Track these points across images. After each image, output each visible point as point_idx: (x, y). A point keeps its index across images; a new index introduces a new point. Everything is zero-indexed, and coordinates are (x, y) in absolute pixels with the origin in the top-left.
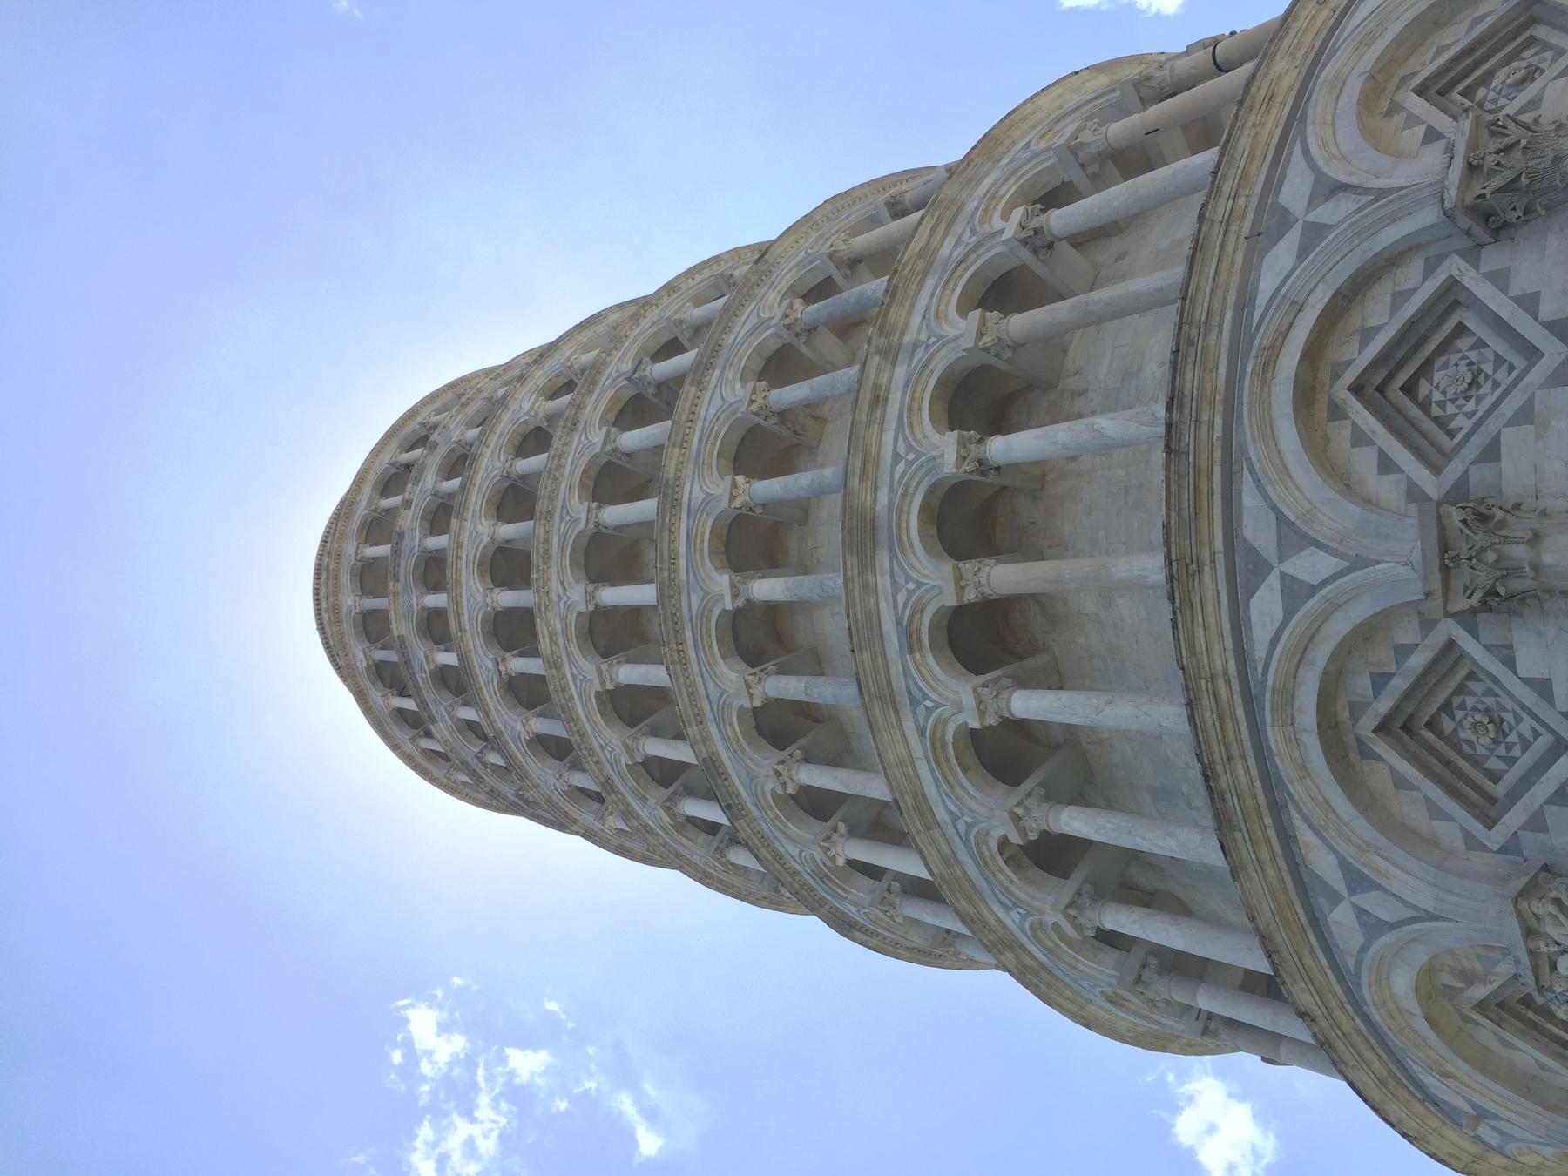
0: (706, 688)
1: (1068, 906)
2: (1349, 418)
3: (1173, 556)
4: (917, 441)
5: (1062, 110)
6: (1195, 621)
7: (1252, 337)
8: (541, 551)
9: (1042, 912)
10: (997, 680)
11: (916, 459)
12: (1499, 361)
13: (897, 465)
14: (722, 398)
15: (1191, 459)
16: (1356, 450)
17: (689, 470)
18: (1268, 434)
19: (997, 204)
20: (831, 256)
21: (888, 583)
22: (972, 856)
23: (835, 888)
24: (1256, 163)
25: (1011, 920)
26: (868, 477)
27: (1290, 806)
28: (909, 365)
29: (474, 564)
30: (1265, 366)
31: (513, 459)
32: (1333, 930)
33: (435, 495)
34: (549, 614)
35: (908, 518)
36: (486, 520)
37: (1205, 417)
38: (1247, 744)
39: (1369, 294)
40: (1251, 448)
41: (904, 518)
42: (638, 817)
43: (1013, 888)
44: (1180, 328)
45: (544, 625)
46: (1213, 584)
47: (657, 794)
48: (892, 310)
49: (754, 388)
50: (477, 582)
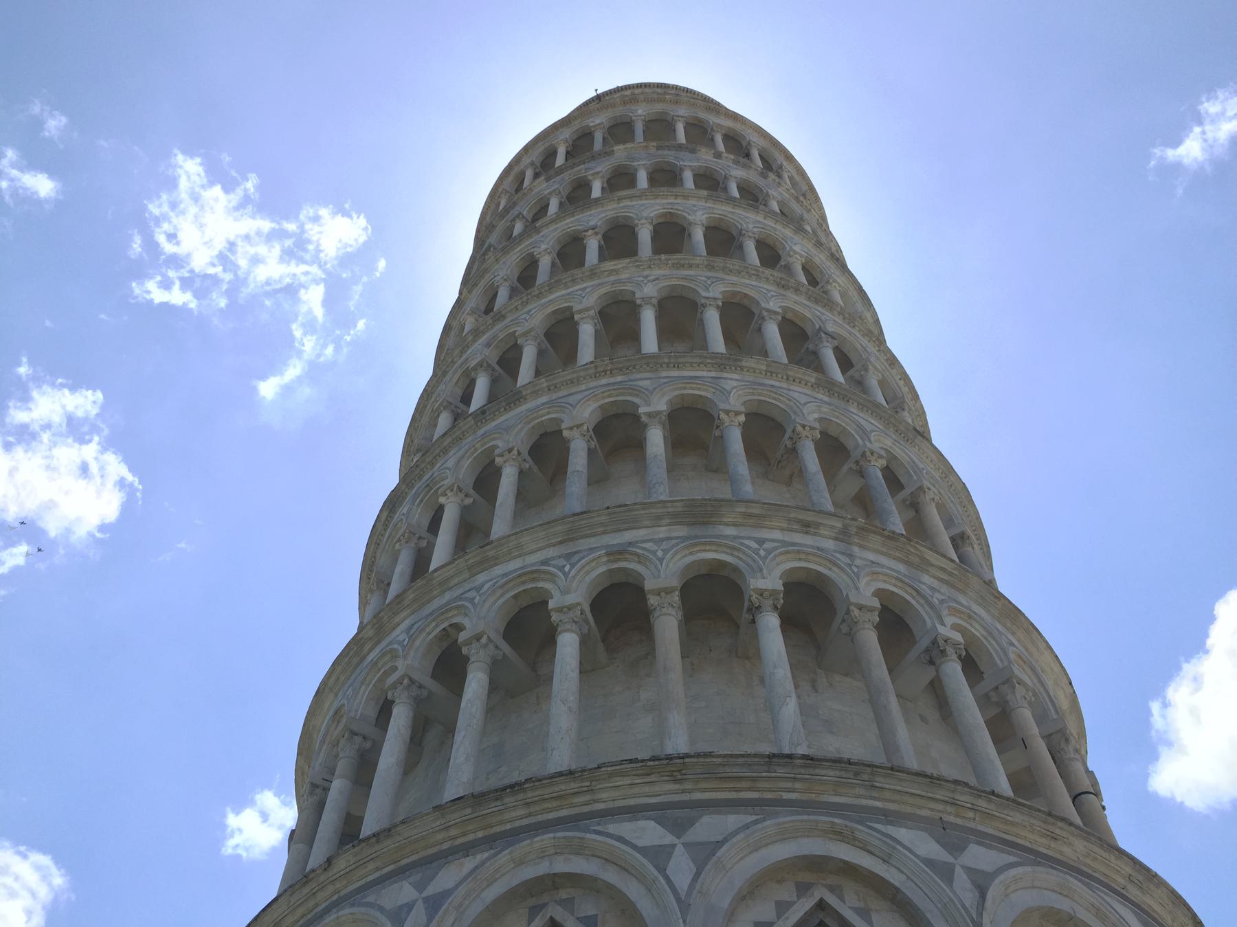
0: (576, 393)
1: (411, 679)
2: (799, 899)
3: (687, 760)
5: (1040, 672)
6: (635, 777)
7: (861, 823)
8: (682, 262)
9: (405, 658)
10: (586, 621)
11: (760, 556)
13: (755, 541)
14: (806, 403)
15: (764, 774)
18: (784, 835)
20: (921, 488)
21: (661, 536)
22: (448, 603)
23: (421, 496)
24: (1002, 826)
25: (399, 633)
26: (745, 519)
27: (492, 852)
28: (835, 551)
29: (672, 209)
31: (755, 238)
32: (396, 886)
33: (726, 178)
35: (714, 551)
36: (706, 218)
37: (798, 785)
38: (540, 818)
41: (713, 548)
42: (474, 341)
43: (424, 634)
44: (869, 766)
45: (624, 265)
46: (665, 791)
47: (492, 355)
48: (879, 537)
49: (815, 429)
50: (657, 212)
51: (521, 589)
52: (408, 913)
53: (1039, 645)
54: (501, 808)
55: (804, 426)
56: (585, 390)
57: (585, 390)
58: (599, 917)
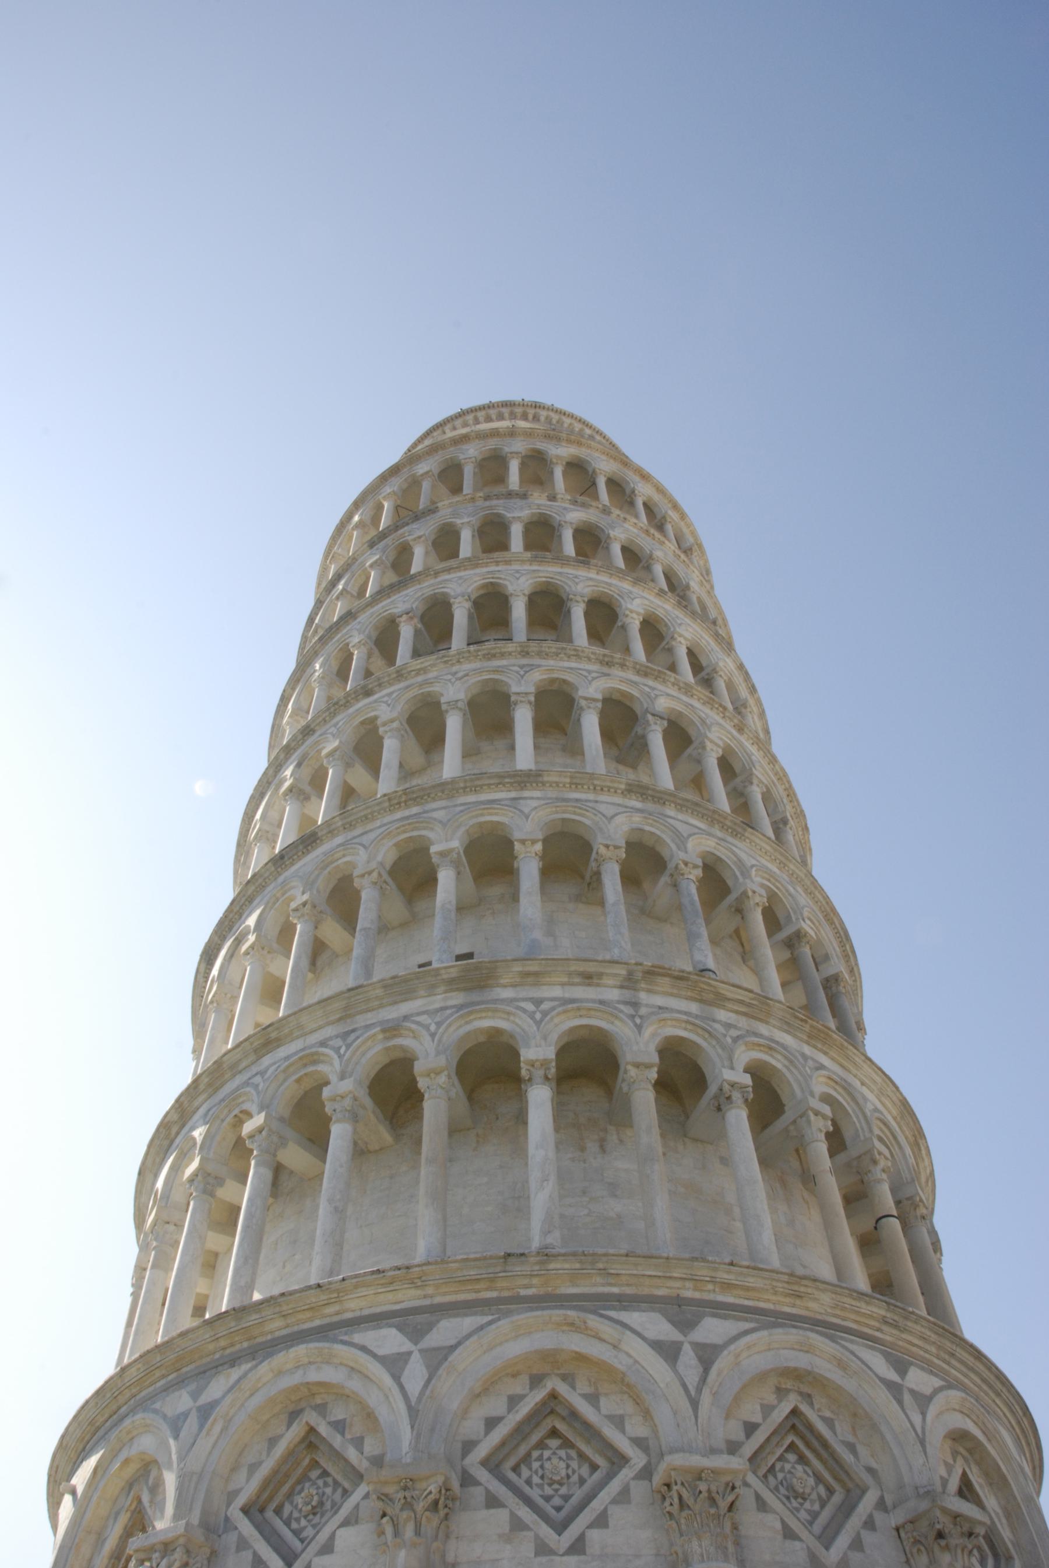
2: (531, 1391)
4: (552, 1019)
12: (566, 1498)
13: (533, 1003)
15: (501, 1275)
16: (505, 1399)
17: (552, 793)
19: (766, 1053)
21: (437, 1006)
24: (741, 1293)
27: (254, 1363)
28: (619, 1002)
30: (572, 1324)
34: (442, 666)
39: (626, 1396)
40: (508, 1320)
41: (490, 1014)
51: (302, 1073)
52: (184, 1421)
53: (857, 1059)
54: (260, 1320)
55: (607, 846)
56: (380, 827)
57: (380, 827)
58: (348, 1421)
